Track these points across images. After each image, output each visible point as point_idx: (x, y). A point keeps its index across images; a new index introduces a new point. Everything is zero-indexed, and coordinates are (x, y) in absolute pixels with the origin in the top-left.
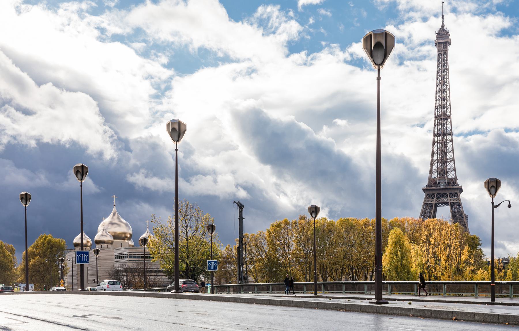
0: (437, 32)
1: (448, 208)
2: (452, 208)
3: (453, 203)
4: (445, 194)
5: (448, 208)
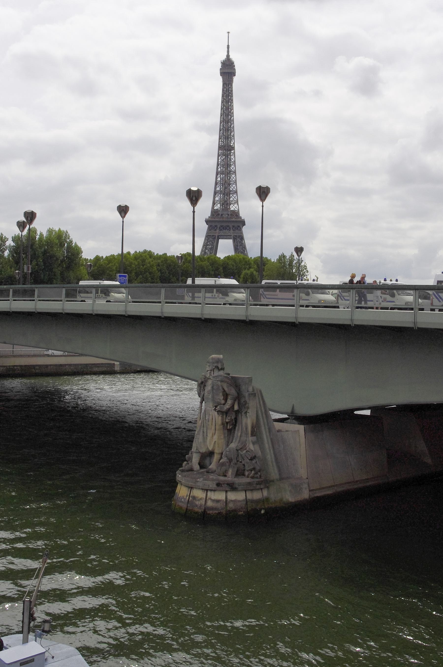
0: (222, 62)
1: (230, 242)
2: (234, 242)
3: (236, 236)
4: (228, 226)
5: (230, 242)
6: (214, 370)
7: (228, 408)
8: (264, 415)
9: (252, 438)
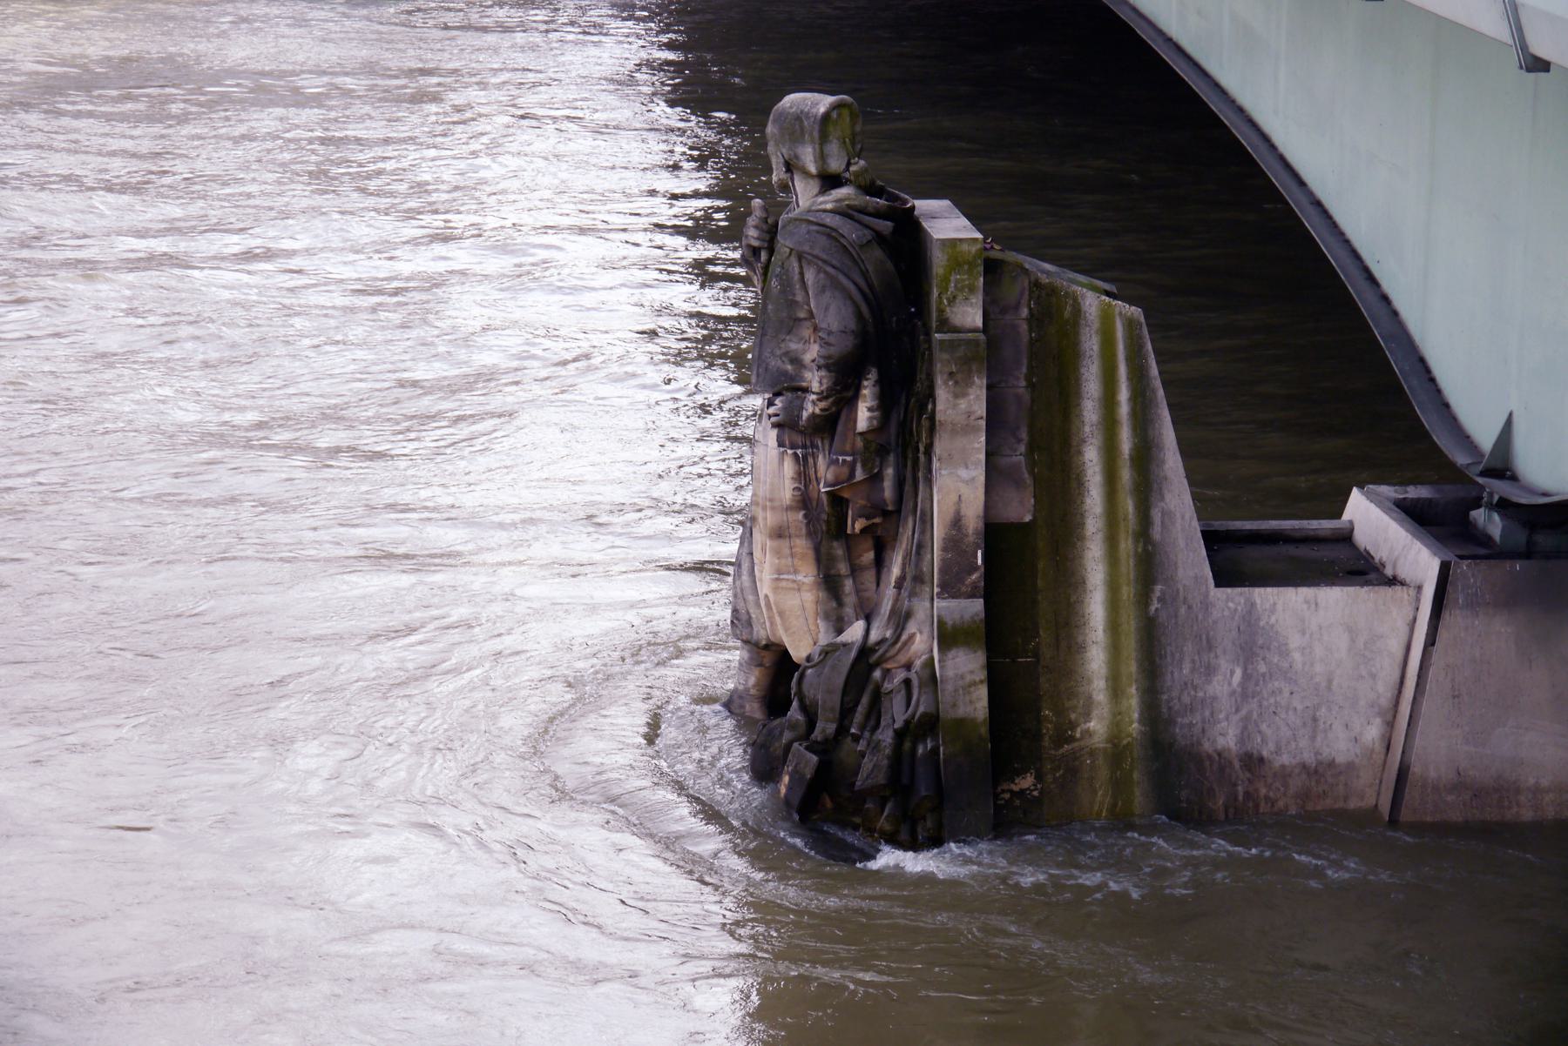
6: (797, 183)
7: (813, 415)
8: (1126, 475)
9: (944, 604)
